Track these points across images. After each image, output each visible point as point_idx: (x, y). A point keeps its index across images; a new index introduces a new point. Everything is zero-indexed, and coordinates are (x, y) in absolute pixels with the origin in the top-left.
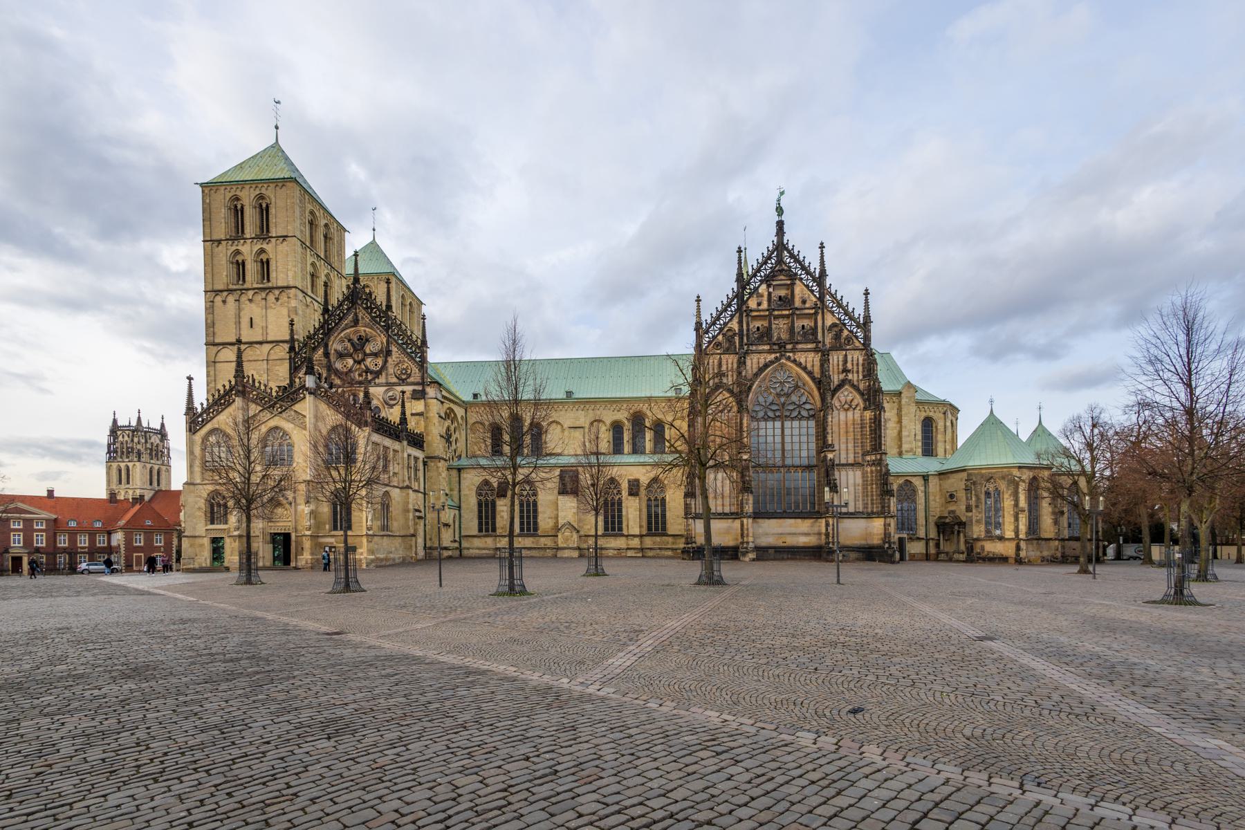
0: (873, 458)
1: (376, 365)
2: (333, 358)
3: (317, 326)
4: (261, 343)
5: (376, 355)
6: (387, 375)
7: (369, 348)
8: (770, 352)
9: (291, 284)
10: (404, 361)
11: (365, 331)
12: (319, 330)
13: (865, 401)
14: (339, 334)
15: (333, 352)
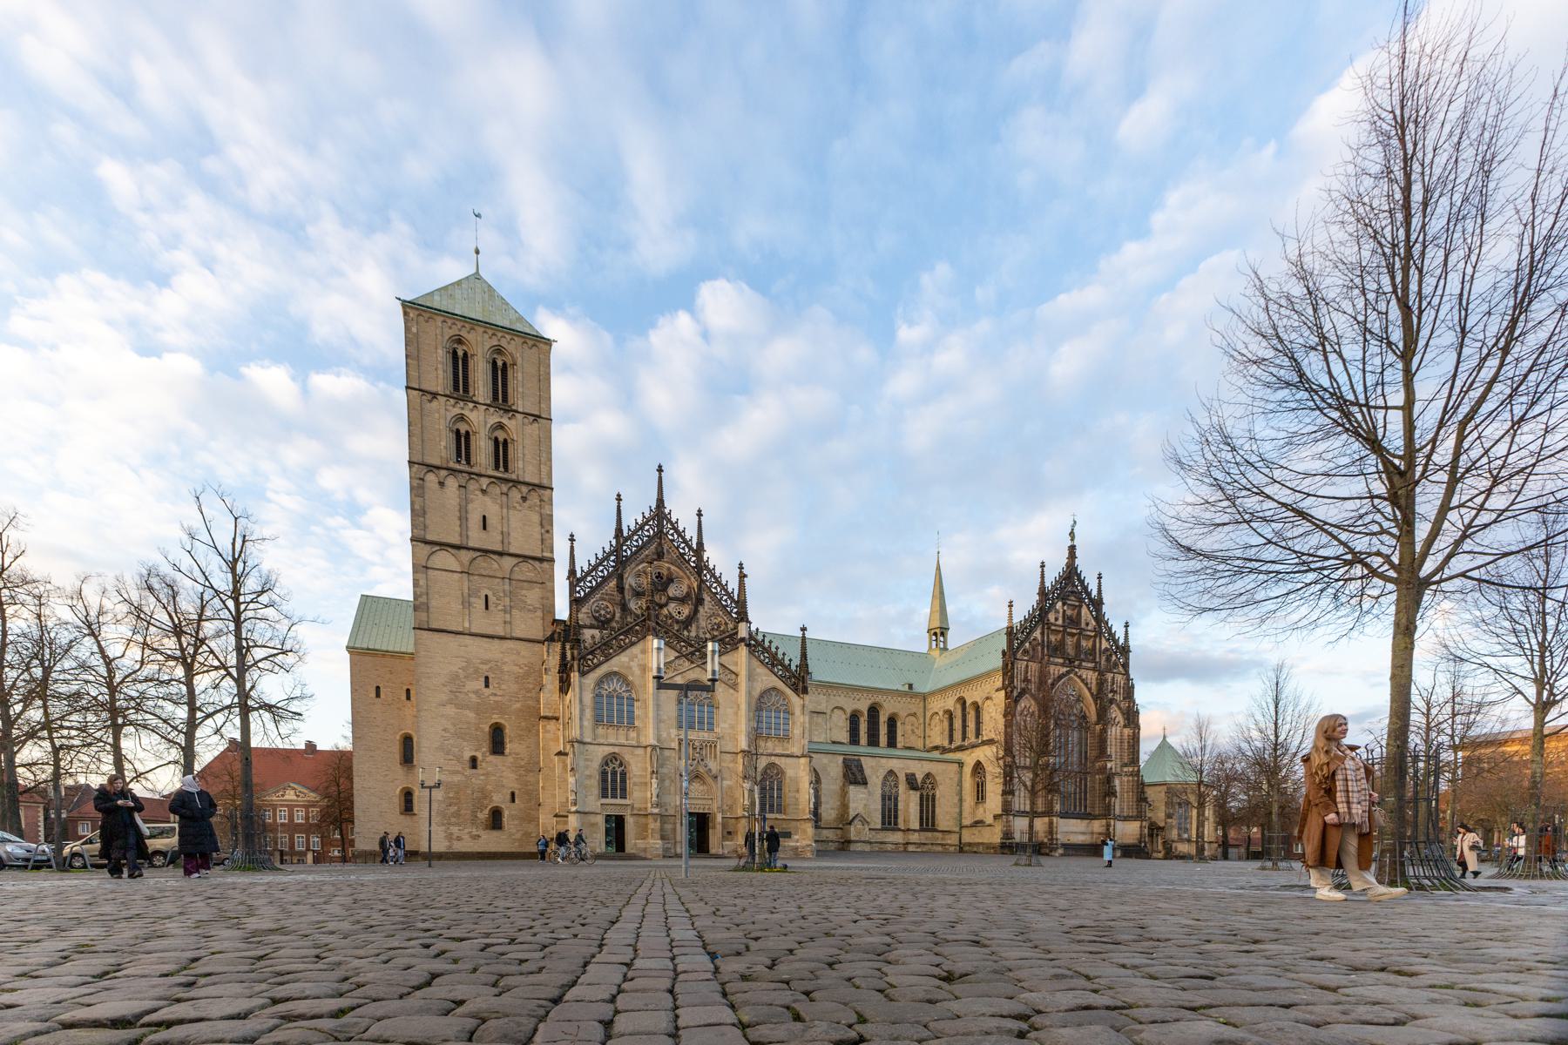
0: (1131, 769)
1: (679, 613)
2: (628, 595)
3: (607, 550)
4: (501, 554)
5: (682, 600)
6: (698, 627)
7: (673, 591)
8: (1063, 665)
9: (545, 482)
10: (719, 615)
11: (669, 569)
12: (610, 554)
13: (1125, 719)
14: (637, 565)
15: (627, 587)
